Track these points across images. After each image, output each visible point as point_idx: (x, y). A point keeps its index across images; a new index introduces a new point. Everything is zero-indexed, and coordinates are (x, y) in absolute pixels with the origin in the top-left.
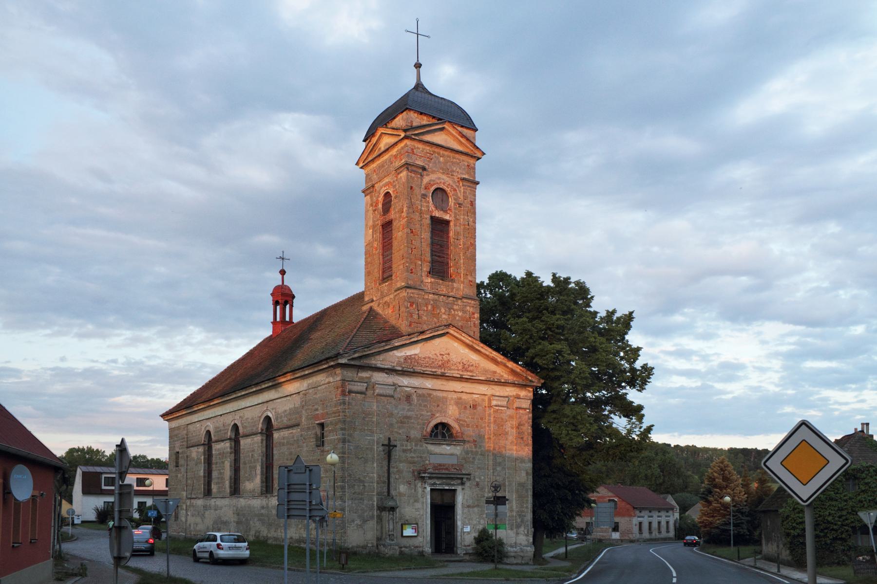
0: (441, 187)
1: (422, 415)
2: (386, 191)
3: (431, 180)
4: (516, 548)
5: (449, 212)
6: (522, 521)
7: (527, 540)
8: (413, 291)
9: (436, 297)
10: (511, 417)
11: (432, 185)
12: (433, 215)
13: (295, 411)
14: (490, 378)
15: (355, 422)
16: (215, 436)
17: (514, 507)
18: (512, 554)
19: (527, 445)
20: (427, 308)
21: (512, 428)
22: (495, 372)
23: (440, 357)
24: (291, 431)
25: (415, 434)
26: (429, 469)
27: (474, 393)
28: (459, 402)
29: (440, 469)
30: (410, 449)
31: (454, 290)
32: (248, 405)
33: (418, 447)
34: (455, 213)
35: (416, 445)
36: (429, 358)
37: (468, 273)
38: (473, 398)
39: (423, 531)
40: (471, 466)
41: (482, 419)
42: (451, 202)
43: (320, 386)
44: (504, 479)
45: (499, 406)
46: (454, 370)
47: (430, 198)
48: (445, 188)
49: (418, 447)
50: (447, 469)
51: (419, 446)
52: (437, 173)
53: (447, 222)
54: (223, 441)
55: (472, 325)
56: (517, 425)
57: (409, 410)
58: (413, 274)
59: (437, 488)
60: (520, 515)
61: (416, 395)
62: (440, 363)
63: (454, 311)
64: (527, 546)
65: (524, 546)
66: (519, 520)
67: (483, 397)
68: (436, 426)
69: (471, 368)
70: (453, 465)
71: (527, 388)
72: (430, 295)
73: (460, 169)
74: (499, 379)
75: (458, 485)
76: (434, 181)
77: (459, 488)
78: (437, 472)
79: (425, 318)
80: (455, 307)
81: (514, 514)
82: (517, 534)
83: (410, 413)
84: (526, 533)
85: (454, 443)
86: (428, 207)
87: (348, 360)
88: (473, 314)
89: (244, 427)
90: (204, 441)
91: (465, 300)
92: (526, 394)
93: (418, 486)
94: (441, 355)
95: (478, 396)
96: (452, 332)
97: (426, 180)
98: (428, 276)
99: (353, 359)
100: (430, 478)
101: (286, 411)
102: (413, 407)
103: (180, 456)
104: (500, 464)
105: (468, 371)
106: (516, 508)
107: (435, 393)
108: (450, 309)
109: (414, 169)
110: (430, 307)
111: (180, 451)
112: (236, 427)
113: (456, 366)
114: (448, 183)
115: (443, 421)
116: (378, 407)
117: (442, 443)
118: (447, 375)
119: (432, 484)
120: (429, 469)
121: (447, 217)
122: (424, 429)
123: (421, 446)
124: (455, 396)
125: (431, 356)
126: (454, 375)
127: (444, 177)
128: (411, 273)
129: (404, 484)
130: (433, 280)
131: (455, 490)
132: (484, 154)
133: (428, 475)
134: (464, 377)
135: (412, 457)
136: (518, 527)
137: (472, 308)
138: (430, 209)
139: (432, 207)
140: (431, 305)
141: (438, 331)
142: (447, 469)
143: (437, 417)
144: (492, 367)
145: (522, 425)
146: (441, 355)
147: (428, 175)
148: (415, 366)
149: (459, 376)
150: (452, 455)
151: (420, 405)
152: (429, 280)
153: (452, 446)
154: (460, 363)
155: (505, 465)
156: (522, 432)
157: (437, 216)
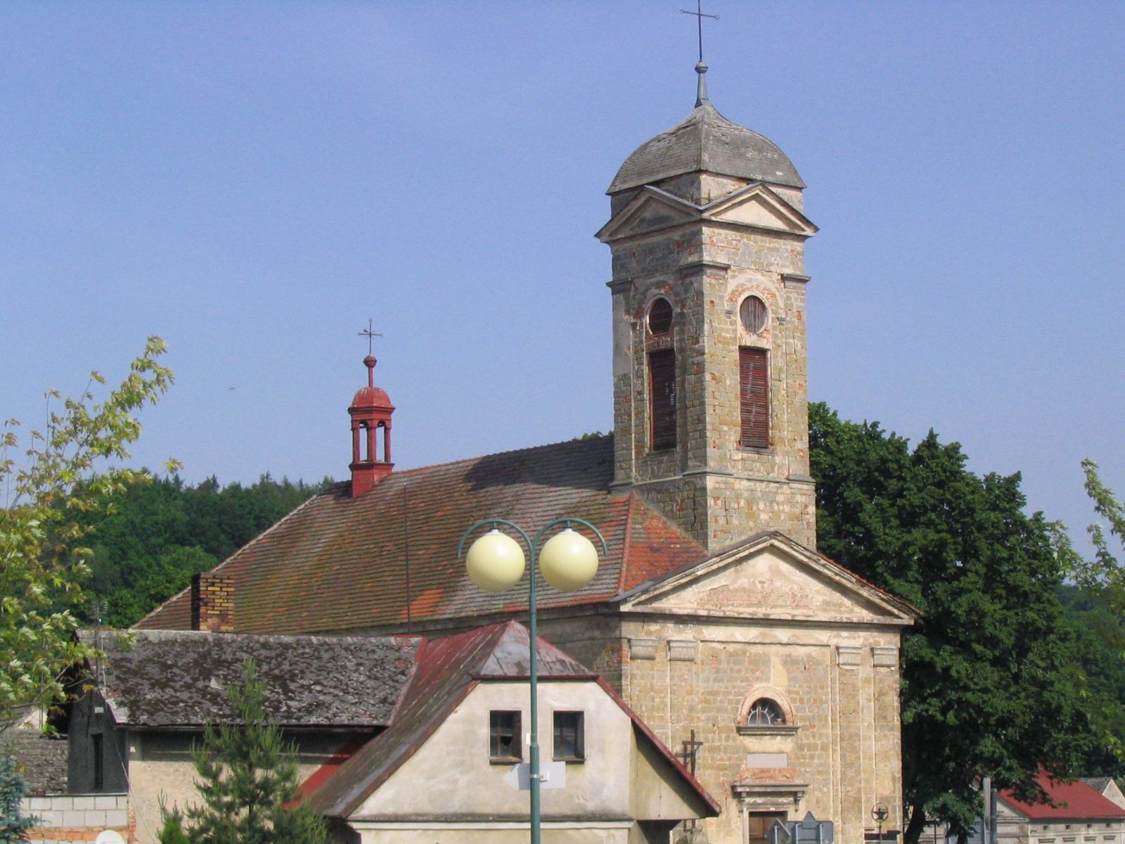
1: (734, 687)
2: (659, 296)
3: (737, 286)
9: (752, 484)
10: (867, 681)
15: (641, 706)
19: (892, 729)
21: (869, 700)
25: (726, 720)
26: (747, 778)
28: (788, 662)
29: (761, 778)
33: (731, 743)
34: (775, 336)
41: (822, 688)
42: (770, 315)
44: (859, 791)
46: (781, 606)
55: (805, 526)
56: (876, 695)
57: (715, 680)
63: (778, 504)
67: (823, 649)
68: (754, 706)
70: (780, 771)
73: (781, 258)
74: (849, 618)
75: (789, 804)
76: (742, 285)
78: (758, 782)
79: (735, 522)
83: (717, 684)
86: (735, 331)
88: (806, 506)
91: (793, 485)
93: (731, 808)
94: (760, 582)
96: (776, 543)
97: (732, 285)
98: (738, 449)
99: (640, 603)
100: (750, 794)
108: (771, 502)
110: (742, 503)
114: (763, 286)
118: (772, 617)
119: (751, 804)
120: (747, 778)
121: (763, 344)
122: (737, 711)
123: (734, 740)
126: (783, 617)
127: (758, 276)
130: (745, 455)
132: (816, 229)
133: (748, 790)
134: (797, 618)
135: (722, 759)
137: (804, 497)
138: (739, 335)
140: (745, 499)
142: (771, 778)
143: (757, 689)
145: (883, 695)
146: (760, 582)
147: (733, 277)
148: (724, 605)
151: (732, 670)
152: (738, 456)
153: (779, 737)
155: (860, 766)
157: (748, 344)
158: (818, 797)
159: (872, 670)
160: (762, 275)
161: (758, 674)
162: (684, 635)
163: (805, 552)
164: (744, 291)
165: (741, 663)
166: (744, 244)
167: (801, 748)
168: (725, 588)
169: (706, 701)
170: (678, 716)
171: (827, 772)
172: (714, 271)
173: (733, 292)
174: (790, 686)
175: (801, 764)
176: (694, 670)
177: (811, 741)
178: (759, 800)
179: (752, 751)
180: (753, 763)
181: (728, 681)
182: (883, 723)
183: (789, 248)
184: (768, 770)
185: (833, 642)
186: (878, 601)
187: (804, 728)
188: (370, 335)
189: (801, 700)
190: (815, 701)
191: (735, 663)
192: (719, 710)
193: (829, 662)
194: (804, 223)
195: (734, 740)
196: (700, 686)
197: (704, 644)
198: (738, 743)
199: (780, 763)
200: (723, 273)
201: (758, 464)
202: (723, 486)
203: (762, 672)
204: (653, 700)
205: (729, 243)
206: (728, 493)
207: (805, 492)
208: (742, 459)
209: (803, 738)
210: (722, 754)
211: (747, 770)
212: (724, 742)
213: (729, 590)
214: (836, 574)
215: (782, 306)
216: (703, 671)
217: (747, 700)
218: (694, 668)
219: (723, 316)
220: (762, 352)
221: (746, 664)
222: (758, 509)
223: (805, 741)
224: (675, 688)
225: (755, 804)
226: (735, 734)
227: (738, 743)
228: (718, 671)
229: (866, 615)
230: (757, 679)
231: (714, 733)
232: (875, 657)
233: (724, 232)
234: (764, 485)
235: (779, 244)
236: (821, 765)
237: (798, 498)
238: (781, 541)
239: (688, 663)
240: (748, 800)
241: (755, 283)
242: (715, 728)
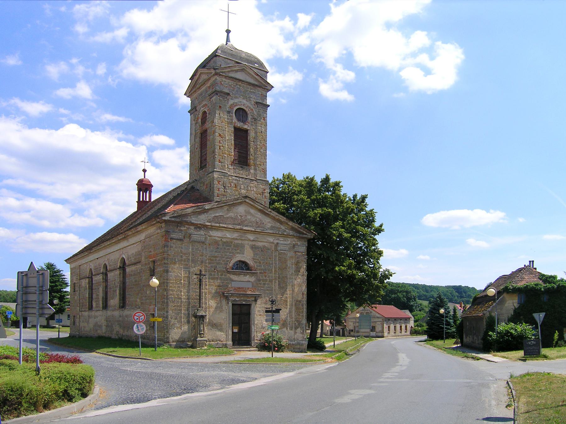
0: (242, 107)
13: (139, 254)
16: (94, 272)
24: (136, 267)
32: (112, 251)
33: (223, 277)
42: (250, 118)
43: (153, 236)
47: (234, 114)
49: (223, 277)
54: (98, 274)
57: (216, 252)
86: (232, 120)
87: (170, 217)
89: (110, 266)
90: (89, 275)
97: (231, 102)
101: (133, 254)
102: (219, 250)
103: (76, 285)
109: (222, 94)
111: (76, 282)
112: (105, 266)
114: (247, 105)
116: (192, 249)
121: (246, 127)
127: (245, 101)
138: (234, 121)
139: (235, 120)
143: (238, 257)
147: (232, 99)
160: (246, 101)
161: (238, 251)
164: (237, 105)
165: (230, 246)
166: (238, 87)
169: (211, 260)
173: (231, 105)
175: (258, 287)
181: (222, 252)
191: (227, 246)
192: (218, 264)
195: (225, 275)
205: (231, 86)
215: (256, 114)
220: (246, 131)
221: (232, 247)
224: (194, 253)
228: (218, 248)
230: (238, 253)
241: (243, 103)
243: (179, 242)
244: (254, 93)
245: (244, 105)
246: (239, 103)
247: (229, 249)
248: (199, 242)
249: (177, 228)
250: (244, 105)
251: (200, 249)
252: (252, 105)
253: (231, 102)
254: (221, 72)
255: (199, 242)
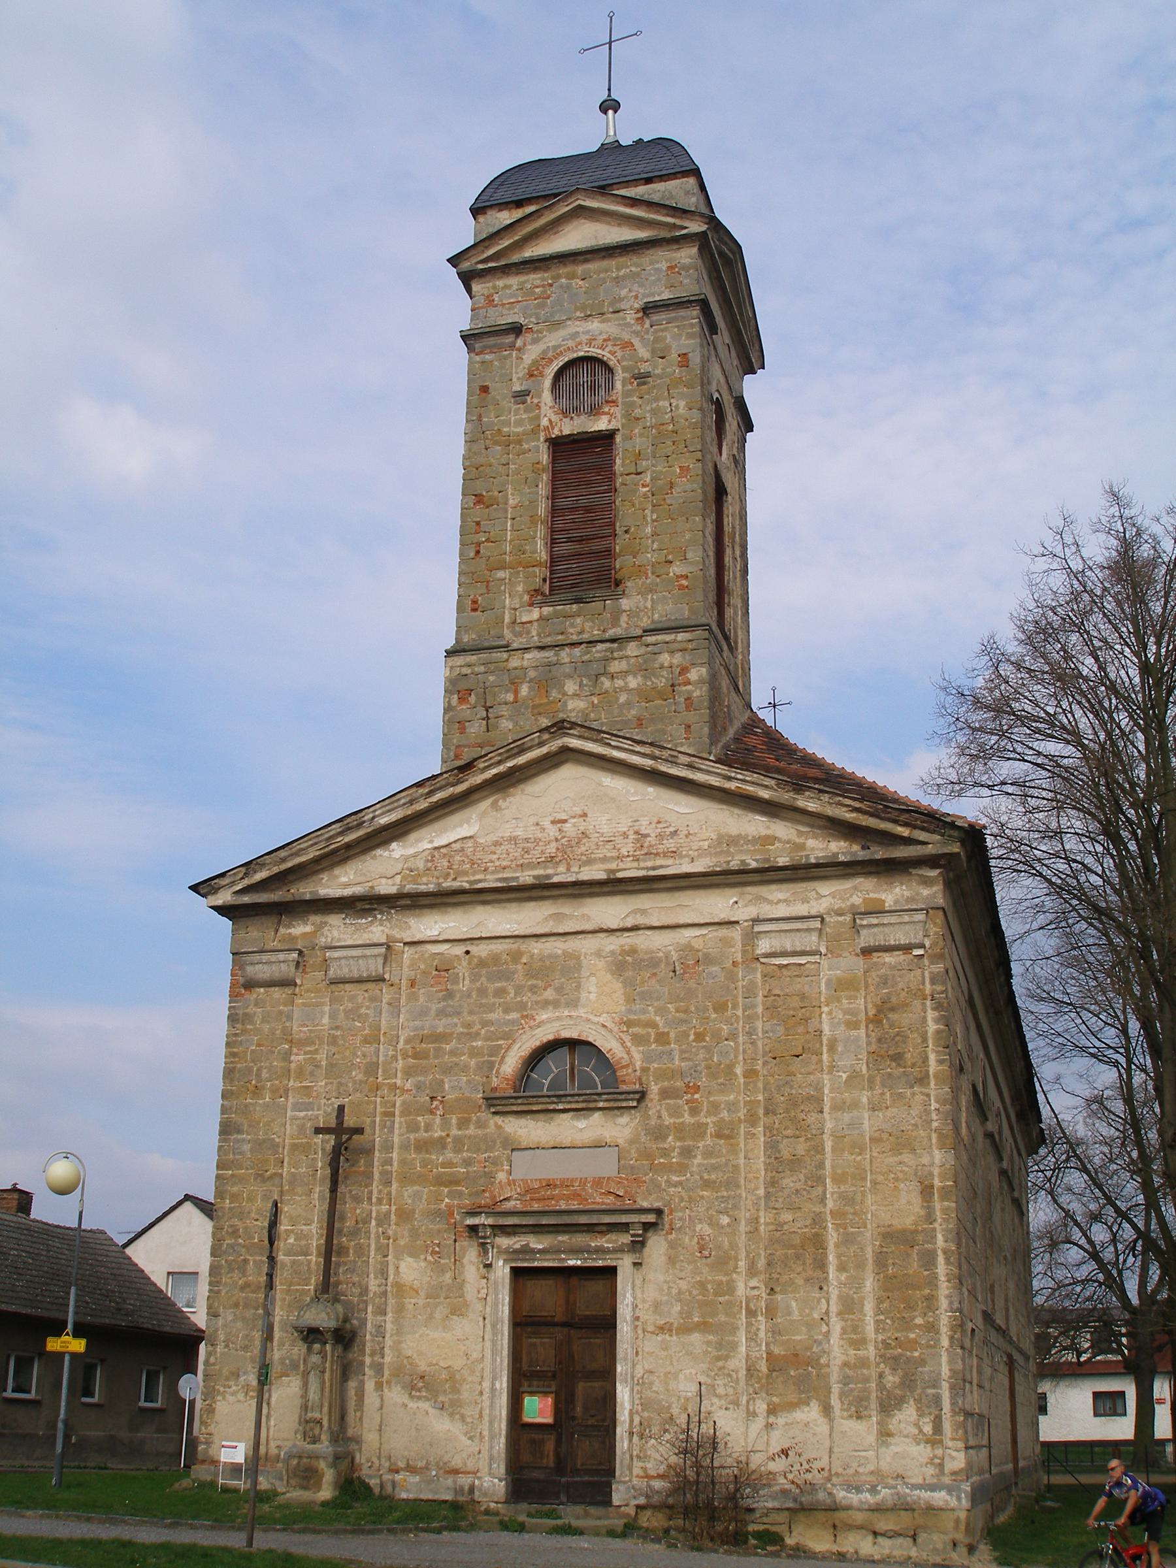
0: (581, 354)
1: (485, 1023)
3: (545, 352)
4: (873, 1490)
5: (606, 410)
6: (908, 1382)
7: (931, 1462)
8: (473, 658)
9: (549, 654)
10: (843, 986)
11: (550, 361)
12: (556, 432)
14: (728, 862)
15: (259, 1070)
17: (870, 1329)
18: (859, 1517)
19: (923, 1080)
20: (516, 692)
22: (770, 840)
23: (553, 831)
27: (681, 922)
30: (441, 1138)
31: (624, 618)
33: (471, 1130)
35: (463, 1123)
36: (513, 840)
37: (670, 557)
38: (683, 941)
39: (481, 1416)
40: (675, 1178)
41: (720, 1008)
45: (784, 954)
48: (594, 351)
49: (471, 1130)
50: (576, 1195)
51: (472, 1127)
52: (569, 323)
53: (608, 437)
56: (872, 1012)
57: (441, 1013)
58: (478, 613)
59: (536, 1264)
60: (895, 1359)
61: (469, 963)
62: (552, 849)
64: (933, 1488)
65: (914, 1487)
66: (891, 1379)
67: (724, 932)
69: (670, 844)
70: (598, 1182)
71: (914, 871)
72: (527, 656)
75: (620, 1250)
76: (555, 347)
77: (624, 1264)
78: (536, 1206)
80: (615, 667)
81: (871, 1352)
82: (885, 1434)
84: (928, 1429)
85: (601, 1104)
88: (684, 670)
91: (651, 639)
92: (907, 894)
93: (465, 1261)
94: (553, 822)
95: (704, 931)
96: (574, 743)
104: (795, 1163)
105: (657, 854)
106: (877, 1331)
107: (536, 947)
113: (609, 846)
115: (566, 1034)
116: (333, 1016)
117: (551, 1107)
119: (516, 1251)
121: (602, 424)
122: (491, 1068)
123: (481, 1125)
124: (613, 944)
125: (520, 833)
127: (594, 325)
128: (474, 610)
129: (413, 1255)
130: (547, 610)
131: (611, 1271)
134: (620, 875)
135: (449, 1164)
136: (889, 1405)
137: (678, 655)
138: (545, 422)
141: (522, 750)
144: (755, 825)
145: (893, 1009)
149: (602, 876)
150: (598, 1145)
151: (482, 992)
152: (535, 614)
153: (597, 1115)
154: (625, 835)
155: (821, 1165)
156: (898, 1034)
157: (566, 432)
158: (701, 1237)
159: (860, 963)
161: (549, 994)
162: (365, 936)
163: (638, 748)
165: (508, 976)
167: (659, 1134)
168: (470, 843)
169: (416, 1056)
170: (340, 1084)
171: (731, 1184)
172: (492, 341)
173: (535, 363)
174: (630, 1011)
176: (386, 998)
177: (687, 1119)
178: (536, 1243)
179: (524, 1144)
180: (528, 1169)
181: (471, 1013)
182: (890, 1068)
183: (664, 266)
184: (566, 1184)
185: (744, 913)
186: (850, 816)
187: (665, 1094)
188: (774, 706)
189: (662, 1038)
190: (700, 1037)
192: (447, 1070)
193: (739, 957)
194: (681, 218)
195: (481, 1125)
196: (406, 1026)
197: (419, 948)
198: (491, 1129)
199: (606, 1166)
200: (509, 339)
201: (578, 620)
202: (482, 669)
203: (560, 990)
204: (286, 1056)
205: (531, 292)
206: (491, 678)
207: (677, 646)
208: (541, 618)
209: (665, 1114)
210: (450, 1155)
211: (510, 1183)
212: (454, 1132)
213: (476, 845)
214: (729, 779)
216: (413, 997)
217: (516, 1047)
218: (387, 995)
219: (508, 403)
221: (519, 977)
222: (565, 694)
223: (668, 1121)
225: (526, 1251)
226: (484, 1115)
227: (491, 1129)
228: (450, 995)
229: (839, 848)
230: (546, 1004)
231: (432, 1113)
232: (864, 932)
233: (514, 281)
234: (577, 651)
235: (637, 265)
236: (715, 1168)
237: (665, 658)
238: (580, 737)
239: (370, 986)
240: (504, 1242)
242: (435, 1103)
243: (276, 993)
244: (634, 276)
245: (589, 343)
246: (571, 344)
247: (500, 992)
248: (360, 981)
249: (277, 931)
250: (589, 343)
251: (363, 1011)
252: (629, 325)
253: (532, 353)
254: (481, 262)
255: (360, 981)
